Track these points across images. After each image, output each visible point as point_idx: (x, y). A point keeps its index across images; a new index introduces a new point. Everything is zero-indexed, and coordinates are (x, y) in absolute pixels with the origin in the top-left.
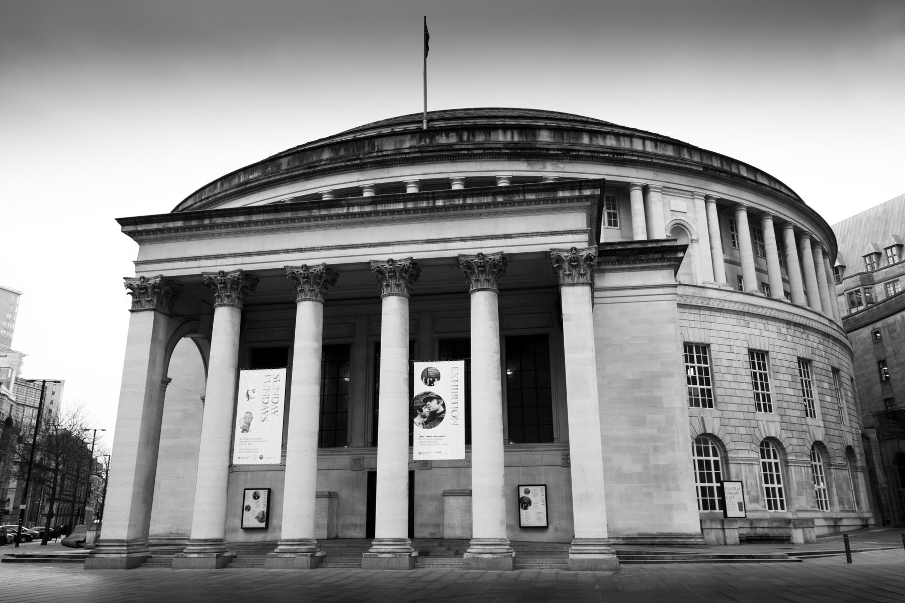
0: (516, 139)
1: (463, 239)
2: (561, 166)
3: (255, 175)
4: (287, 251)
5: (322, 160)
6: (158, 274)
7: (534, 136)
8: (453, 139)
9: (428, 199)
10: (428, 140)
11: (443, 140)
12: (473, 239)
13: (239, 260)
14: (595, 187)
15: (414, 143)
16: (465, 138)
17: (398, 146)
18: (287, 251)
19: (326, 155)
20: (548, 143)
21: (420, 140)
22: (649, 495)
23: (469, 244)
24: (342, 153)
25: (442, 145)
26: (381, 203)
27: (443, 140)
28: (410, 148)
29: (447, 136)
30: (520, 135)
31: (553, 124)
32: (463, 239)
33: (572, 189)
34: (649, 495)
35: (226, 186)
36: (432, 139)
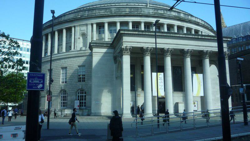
0: (176, 15)
1: (203, 46)
2: (187, 24)
3: (103, 11)
4: (163, 44)
5: (126, 11)
6: (131, 45)
7: (180, 15)
8: (162, 12)
9: (197, 36)
10: (156, 11)
11: (160, 12)
12: (205, 46)
13: (151, 44)
14: (230, 39)
15: (153, 11)
16: (165, 12)
17: (149, 11)
18: (163, 44)
19: (127, 10)
20: (182, 17)
21: (154, 10)
22: (216, 103)
23: (204, 47)
24: (132, 10)
25: (160, 13)
26: (187, 35)
27: (160, 12)
28: (152, 13)
29: (161, 11)
30: (177, 14)
31: (184, 13)
32: (203, 46)
33: (226, 38)
34: (216, 103)
35: (90, 13)
36: (157, 11)
